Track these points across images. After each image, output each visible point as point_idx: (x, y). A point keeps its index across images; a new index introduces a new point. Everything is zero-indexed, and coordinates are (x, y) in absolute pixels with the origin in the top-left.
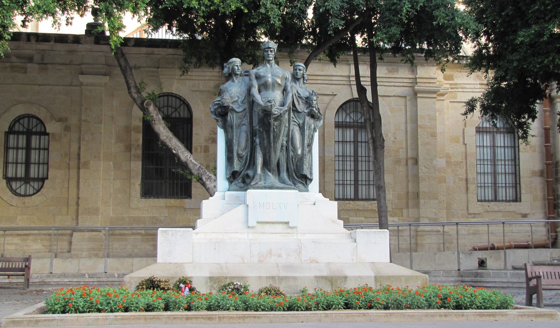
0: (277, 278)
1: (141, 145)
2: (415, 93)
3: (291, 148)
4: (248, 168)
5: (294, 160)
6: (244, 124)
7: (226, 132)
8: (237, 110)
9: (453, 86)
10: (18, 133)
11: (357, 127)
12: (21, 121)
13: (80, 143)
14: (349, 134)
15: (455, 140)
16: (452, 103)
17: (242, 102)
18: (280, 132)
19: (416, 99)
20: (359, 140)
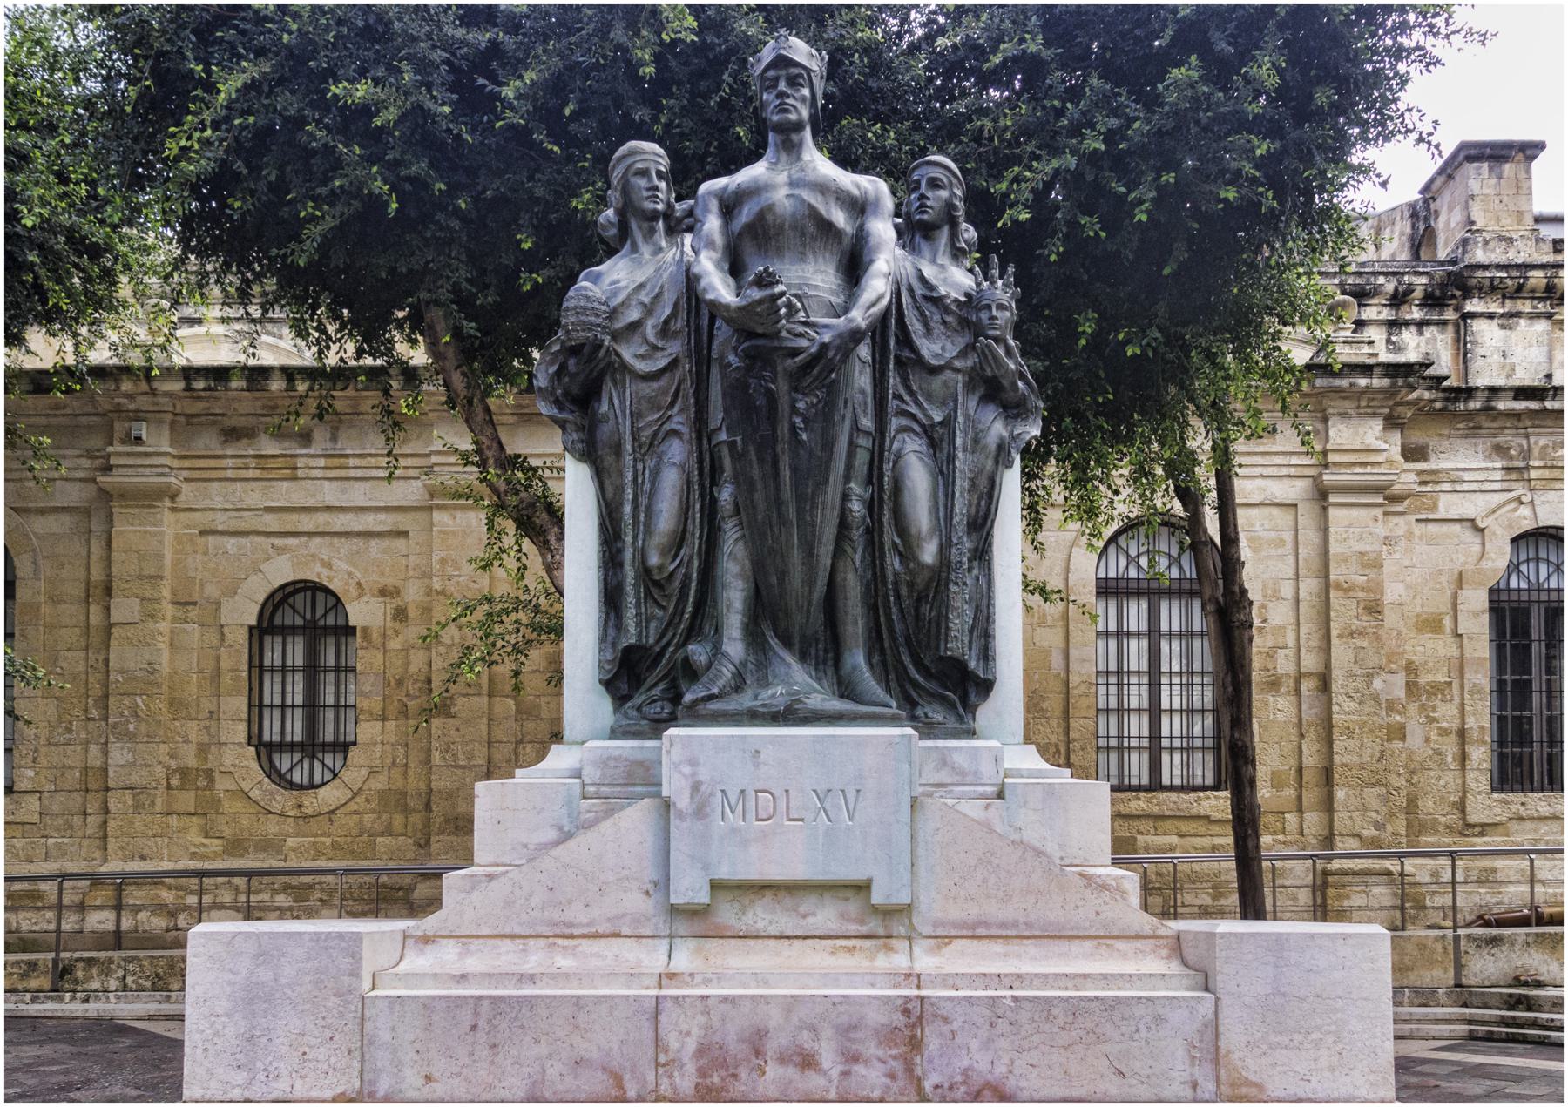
2: (1322, 494)
3: (890, 536)
5: (904, 591)
6: (675, 433)
7: (599, 475)
8: (642, 367)
9: (1426, 478)
10: (285, 631)
12: (291, 600)
14: (1136, 614)
15: (1431, 625)
16: (1422, 525)
17: (665, 331)
18: (829, 445)
19: (1325, 509)
20: (1164, 626)
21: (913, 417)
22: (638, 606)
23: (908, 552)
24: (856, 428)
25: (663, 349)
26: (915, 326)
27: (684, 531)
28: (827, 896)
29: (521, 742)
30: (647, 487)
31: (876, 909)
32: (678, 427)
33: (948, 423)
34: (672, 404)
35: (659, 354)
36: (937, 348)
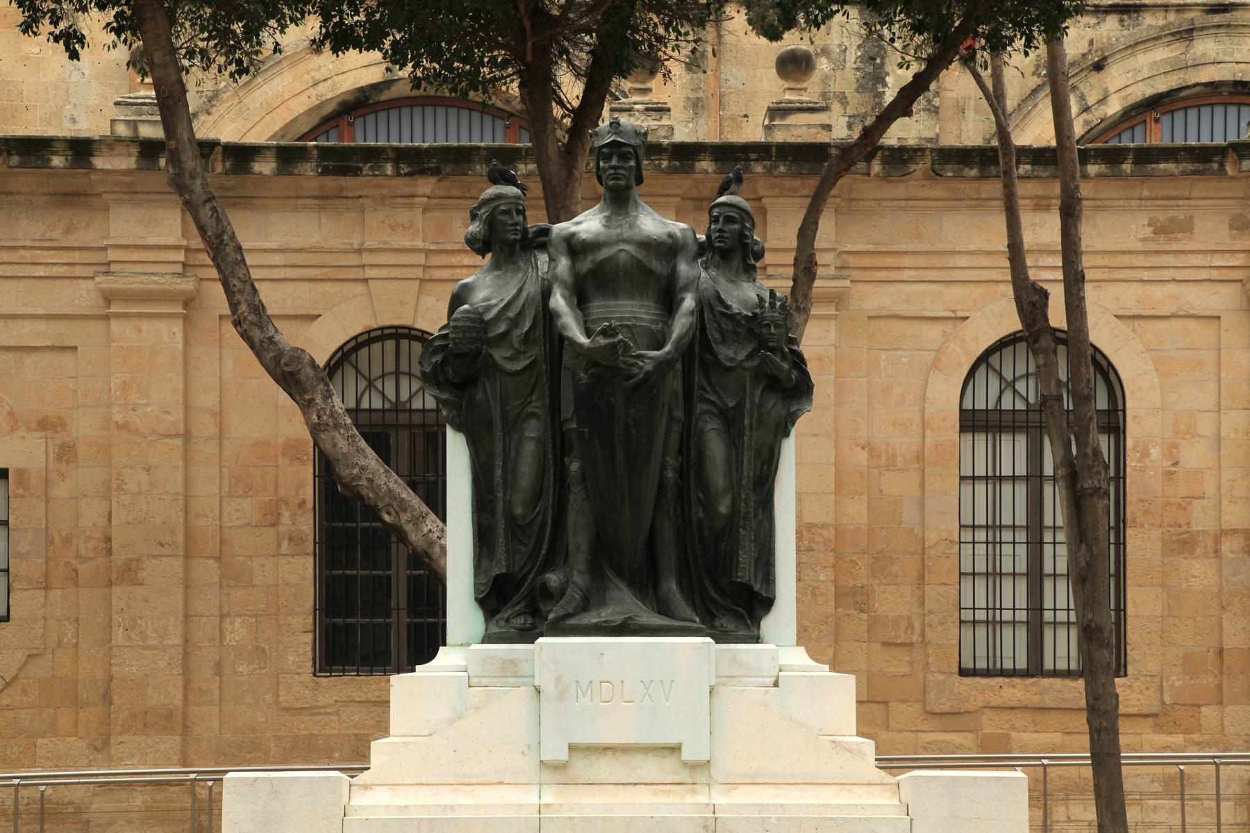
1: (310, 504)
4: (548, 565)
6: (533, 415)
11: (1029, 423)
13: (108, 499)
14: (1013, 453)
17: (527, 339)
21: (713, 403)
22: (507, 544)
23: (709, 504)
24: (671, 418)
25: (525, 352)
26: (714, 335)
27: (542, 489)
28: (650, 755)
29: (228, 615)
30: (513, 454)
31: (685, 764)
32: (536, 411)
33: (739, 407)
34: (531, 393)
35: (522, 357)
36: (730, 353)
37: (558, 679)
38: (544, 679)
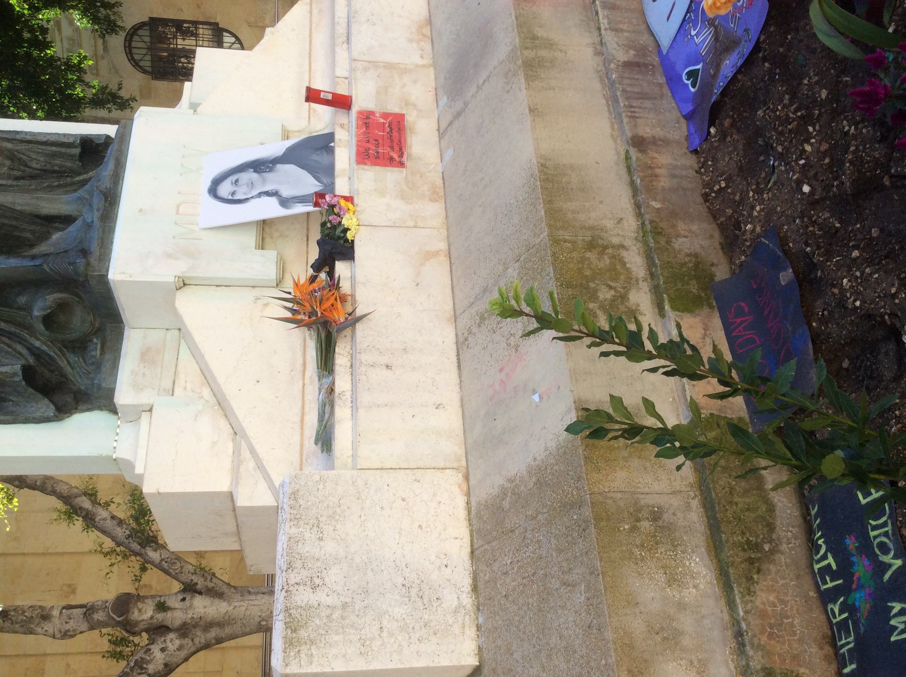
0: (529, 54)
37: (169, 256)
38: (167, 273)
